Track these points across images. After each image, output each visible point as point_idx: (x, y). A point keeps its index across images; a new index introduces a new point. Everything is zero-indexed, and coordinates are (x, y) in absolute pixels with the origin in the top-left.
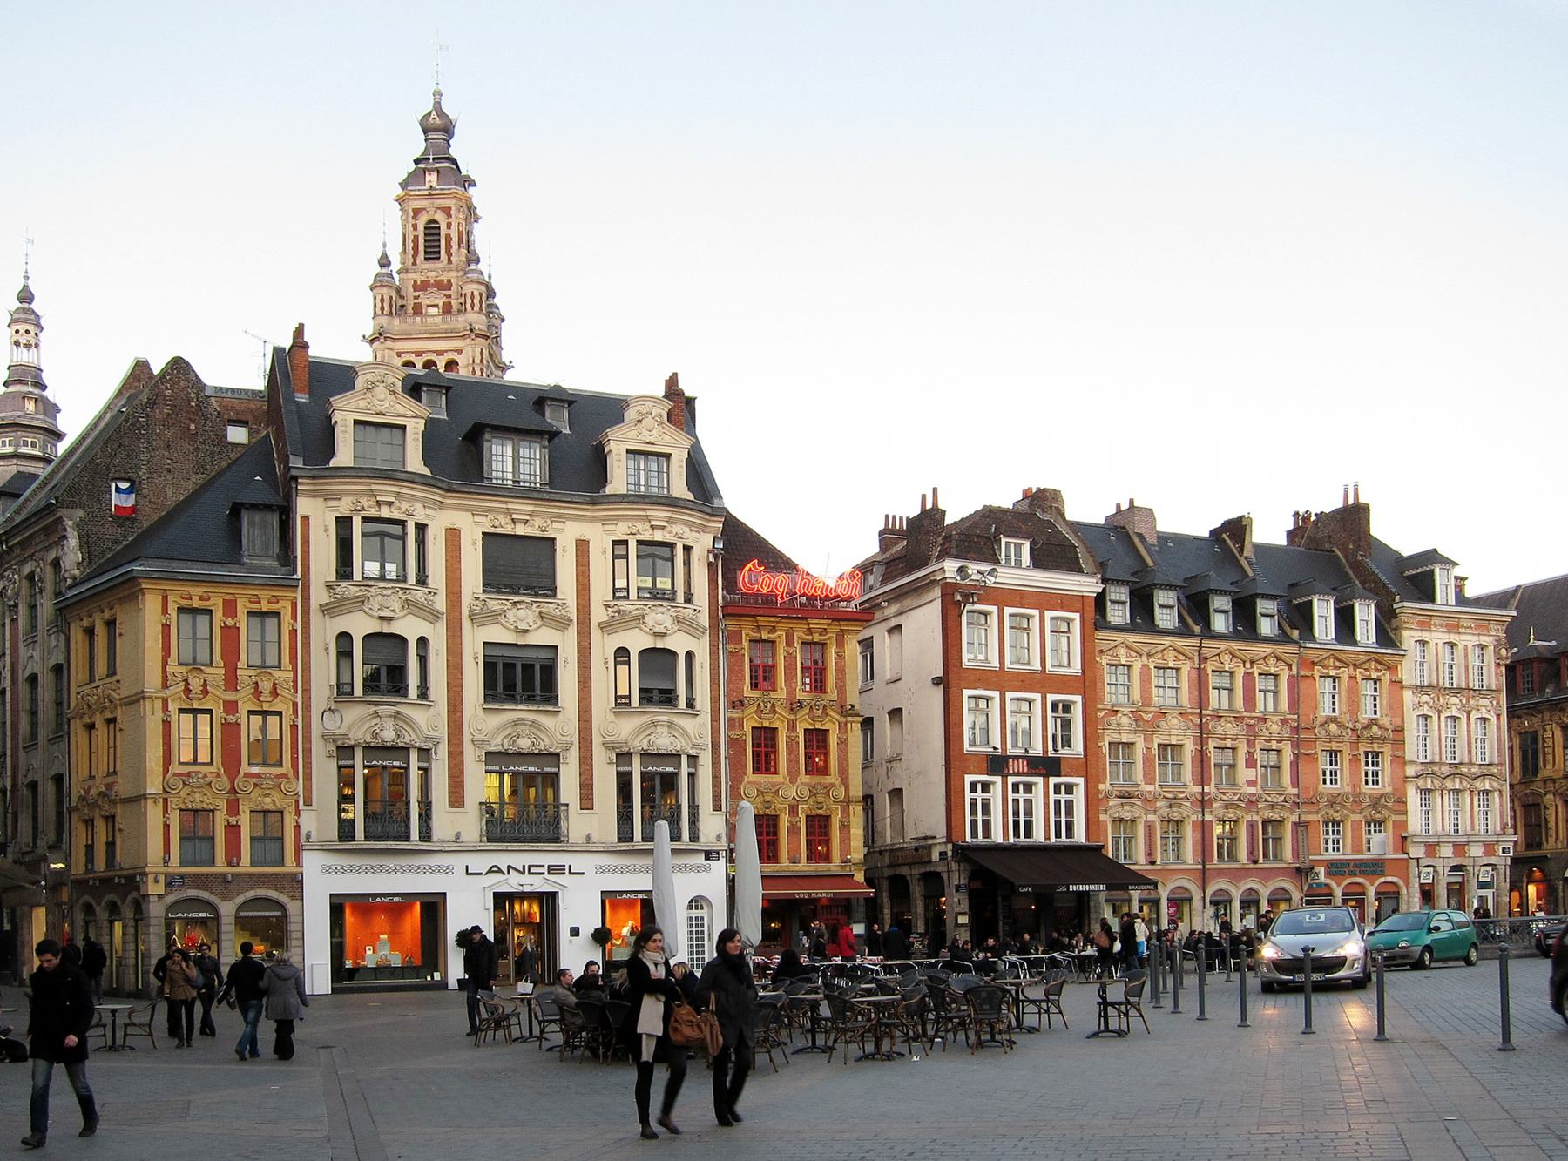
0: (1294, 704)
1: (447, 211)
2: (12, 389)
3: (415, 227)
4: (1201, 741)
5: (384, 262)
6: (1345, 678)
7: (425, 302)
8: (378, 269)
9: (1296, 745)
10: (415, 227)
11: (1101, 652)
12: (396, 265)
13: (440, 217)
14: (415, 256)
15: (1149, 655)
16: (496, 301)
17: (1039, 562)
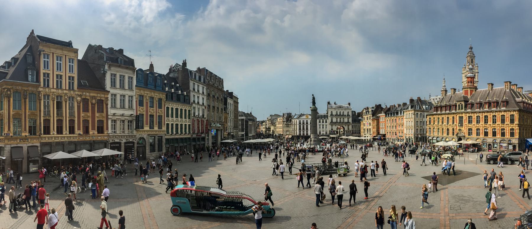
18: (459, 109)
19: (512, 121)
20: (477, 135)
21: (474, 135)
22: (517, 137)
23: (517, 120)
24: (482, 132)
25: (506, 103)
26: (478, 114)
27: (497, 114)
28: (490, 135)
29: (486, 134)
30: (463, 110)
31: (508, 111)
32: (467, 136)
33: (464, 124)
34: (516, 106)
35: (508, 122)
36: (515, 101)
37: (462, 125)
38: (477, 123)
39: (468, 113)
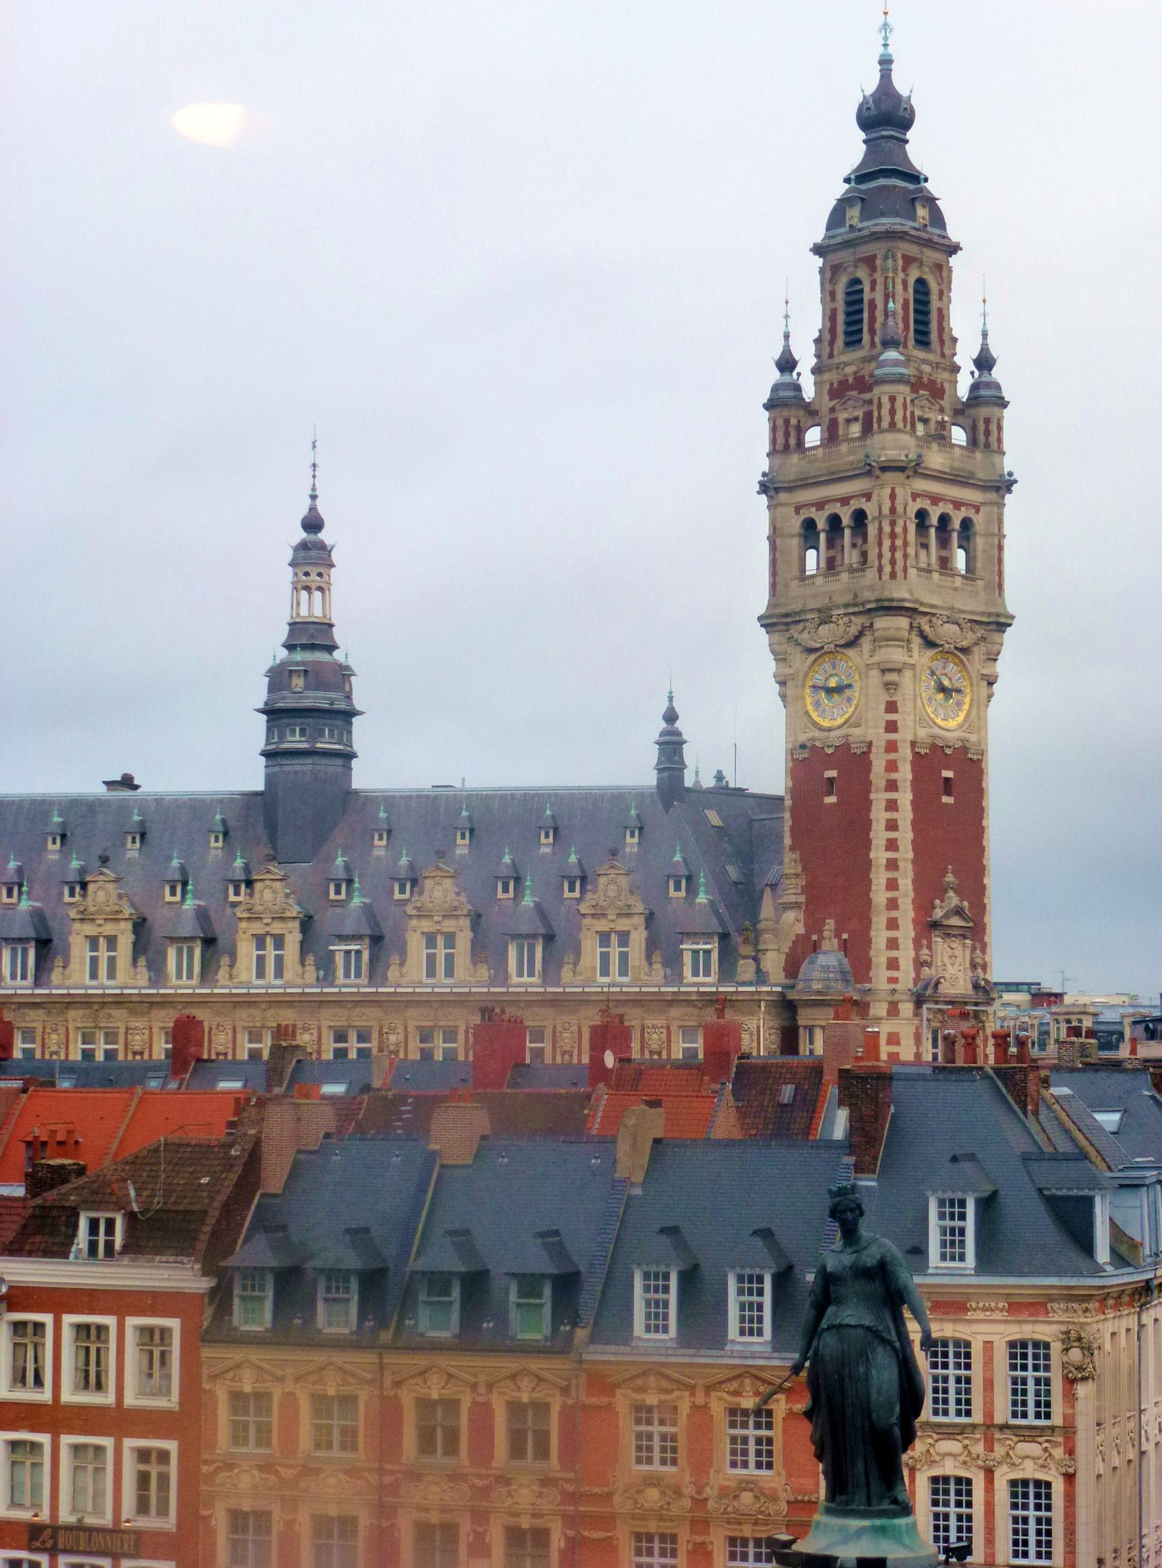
0: (570, 1452)
1: (870, 262)
2: (299, 656)
3: (833, 294)
4: (384, 1509)
5: (787, 364)
6: (685, 1408)
7: (842, 416)
8: (775, 375)
9: (570, 1520)
10: (833, 294)
11: (214, 1378)
12: (806, 358)
13: (862, 273)
14: (832, 342)
15: (298, 1379)
16: (997, 374)
17: (133, 1247)
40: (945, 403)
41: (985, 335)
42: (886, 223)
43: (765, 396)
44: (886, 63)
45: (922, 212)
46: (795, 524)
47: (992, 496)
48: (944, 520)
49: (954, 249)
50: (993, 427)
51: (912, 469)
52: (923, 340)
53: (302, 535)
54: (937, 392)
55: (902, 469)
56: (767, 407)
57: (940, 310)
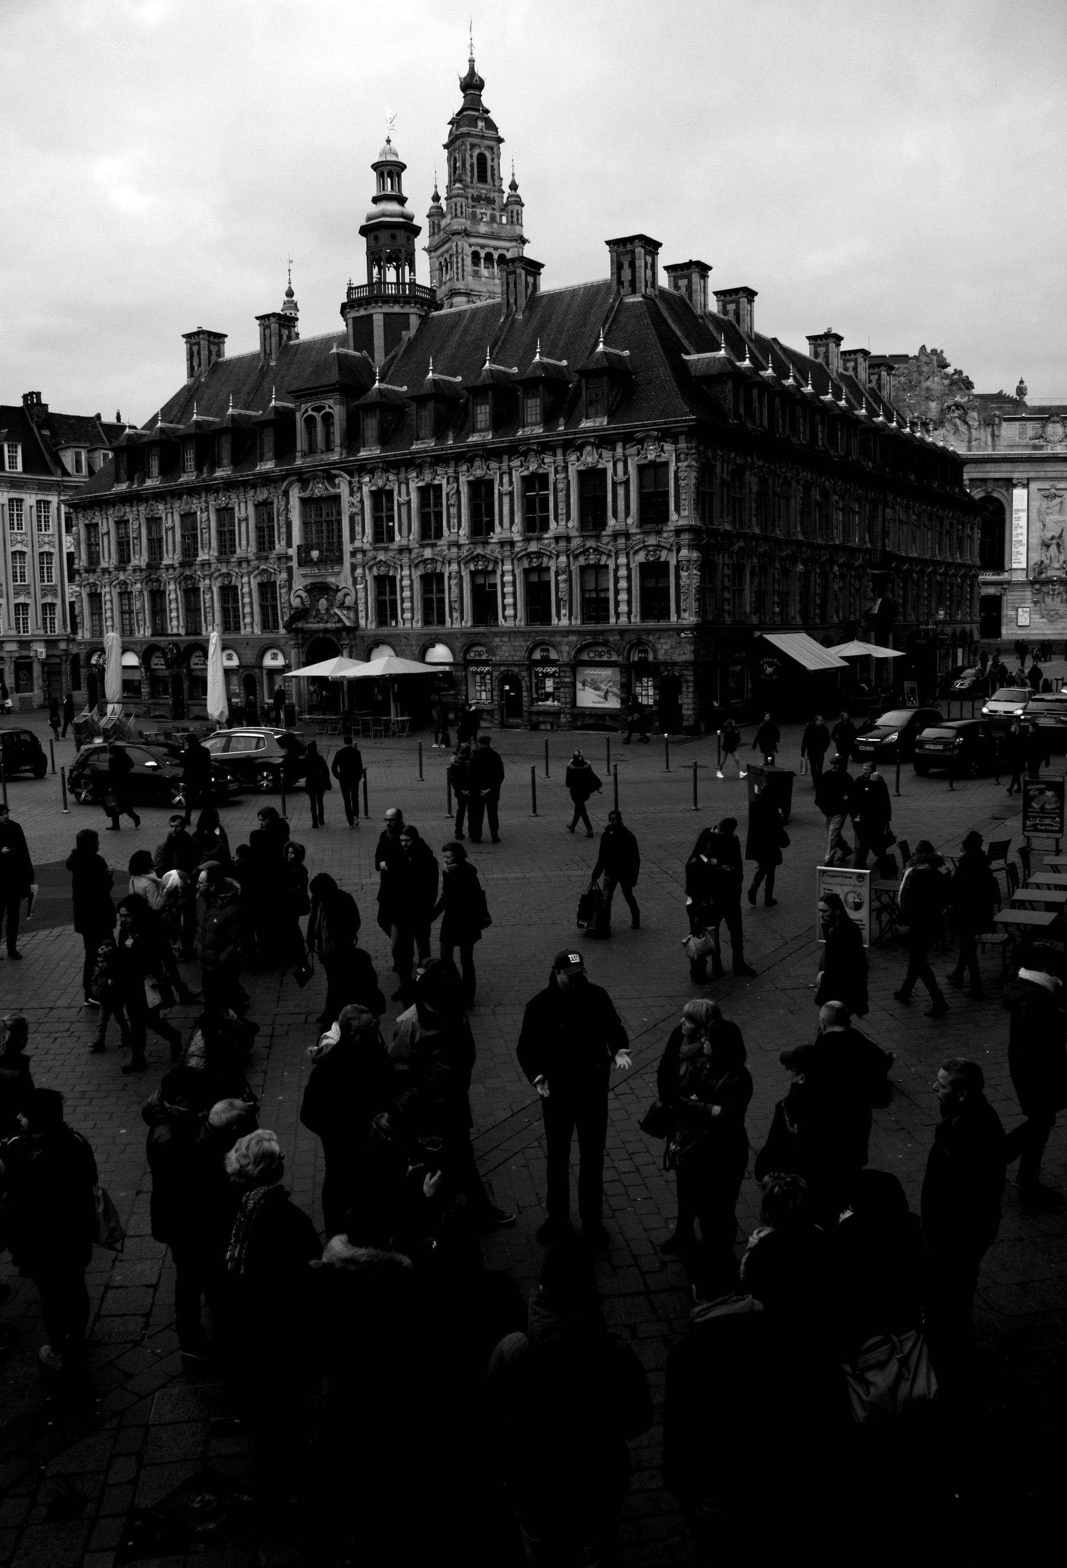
5: (436, 198)
8: (431, 203)
12: (443, 193)
16: (519, 192)
18: (311, 450)
19: (653, 510)
20: (427, 621)
21: (410, 619)
22: (690, 618)
23: (688, 498)
24: (458, 591)
25: (617, 385)
26: (428, 477)
27: (549, 463)
28: (511, 611)
29: (485, 604)
30: (335, 457)
31: (628, 439)
32: (367, 623)
33: (347, 548)
34: (680, 402)
35: (623, 515)
36: (681, 369)
37: (333, 556)
38: (425, 533)
39: (363, 468)
40: (496, 206)
41: (513, 175)
42: (464, 130)
43: (427, 212)
44: (472, 61)
45: (481, 124)
46: (437, 266)
47: (514, 244)
48: (489, 257)
49: (500, 140)
50: (515, 214)
51: (467, 233)
52: (482, 178)
53: (286, 299)
54: (490, 201)
55: (460, 233)
56: (428, 216)
57: (492, 167)
